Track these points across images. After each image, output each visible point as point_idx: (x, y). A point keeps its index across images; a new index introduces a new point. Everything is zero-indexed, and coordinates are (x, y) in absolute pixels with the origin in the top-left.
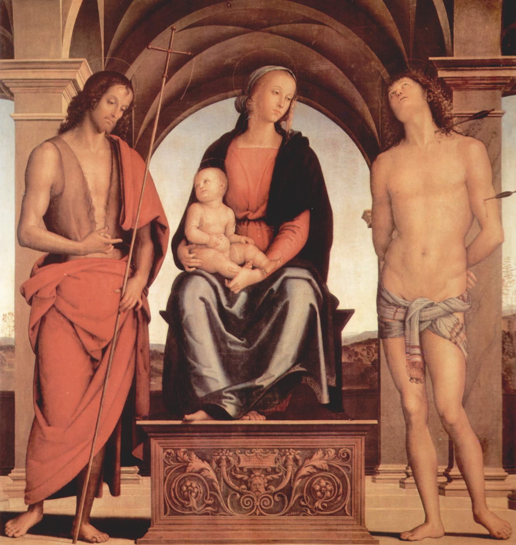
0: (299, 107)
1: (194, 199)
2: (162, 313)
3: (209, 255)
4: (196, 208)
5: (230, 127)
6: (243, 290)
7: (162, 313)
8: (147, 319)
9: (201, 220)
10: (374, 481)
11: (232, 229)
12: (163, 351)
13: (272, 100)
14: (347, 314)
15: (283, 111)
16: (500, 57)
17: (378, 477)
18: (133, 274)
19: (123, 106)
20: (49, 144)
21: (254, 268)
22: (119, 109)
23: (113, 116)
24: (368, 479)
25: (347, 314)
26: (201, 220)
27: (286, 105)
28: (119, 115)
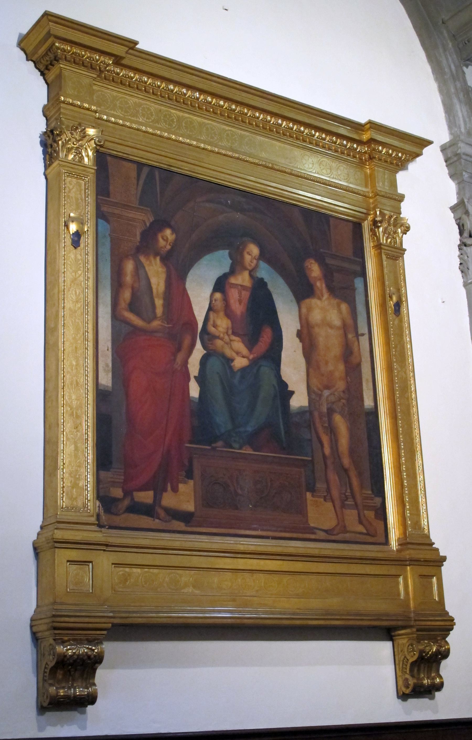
0: (263, 265)
1: (210, 309)
2: (195, 377)
3: (219, 343)
4: (212, 315)
5: (226, 268)
6: (238, 370)
7: (195, 377)
8: (189, 380)
9: (214, 322)
10: (313, 496)
11: (230, 332)
12: (197, 401)
13: (248, 258)
14: (292, 393)
15: (253, 265)
16: (352, 258)
17: (315, 494)
18: (179, 349)
19: (170, 243)
20: (130, 257)
21: (243, 357)
22: (168, 243)
23: (165, 247)
24: (309, 495)
25: (292, 393)
26: (214, 322)
27: (255, 262)
28: (169, 247)
